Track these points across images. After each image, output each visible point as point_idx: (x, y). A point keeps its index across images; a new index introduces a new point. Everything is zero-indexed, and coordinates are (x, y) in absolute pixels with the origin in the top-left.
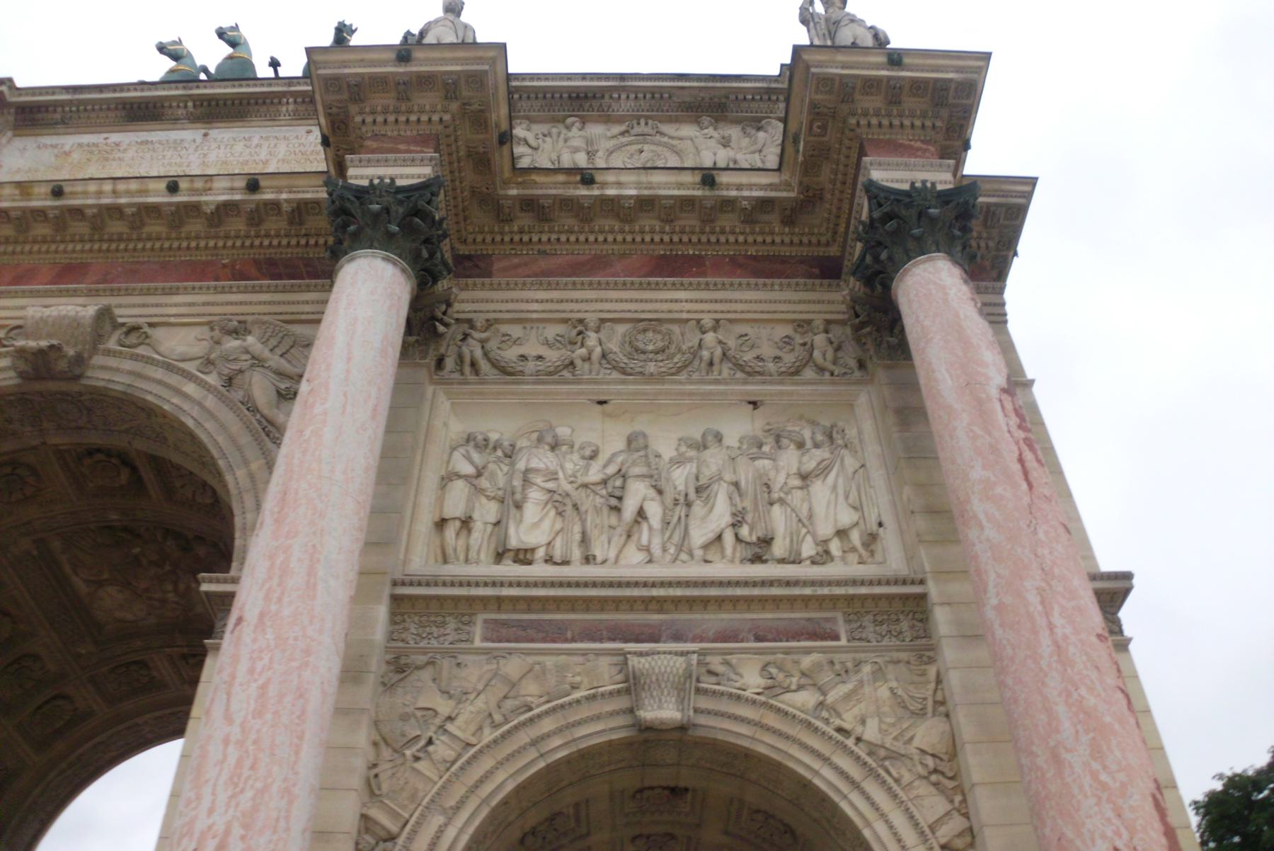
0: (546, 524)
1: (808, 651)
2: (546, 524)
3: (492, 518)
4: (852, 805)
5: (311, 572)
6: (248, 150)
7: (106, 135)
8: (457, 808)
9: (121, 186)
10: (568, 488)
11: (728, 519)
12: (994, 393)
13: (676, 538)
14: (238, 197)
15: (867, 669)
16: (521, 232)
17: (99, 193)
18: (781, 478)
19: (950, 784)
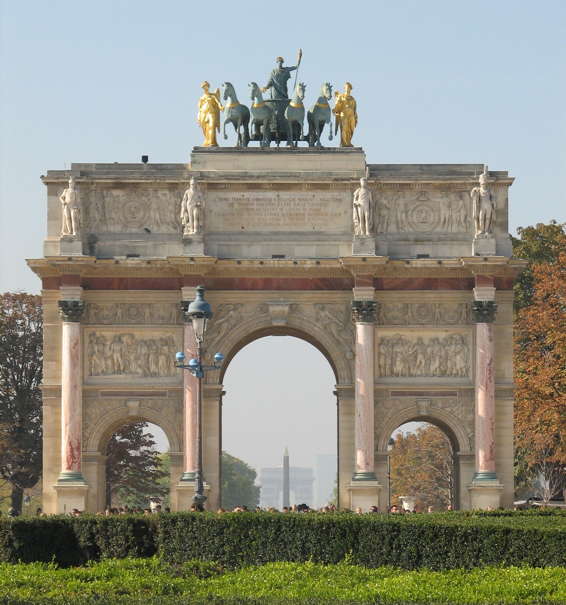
0: (401, 365)
1: (451, 399)
2: (401, 365)
3: (389, 363)
4: (455, 430)
5: (369, 406)
6: (296, 207)
7: (242, 194)
8: (390, 429)
9: (280, 262)
10: (405, 355)
11: (438, 365)
12: (486, 365)
13: (428, 367)
14: (314, 266)
15: (461, 403)
16: (390, 272)
17: (274, 264)
18: (450, 354)
19: (472, 427)
